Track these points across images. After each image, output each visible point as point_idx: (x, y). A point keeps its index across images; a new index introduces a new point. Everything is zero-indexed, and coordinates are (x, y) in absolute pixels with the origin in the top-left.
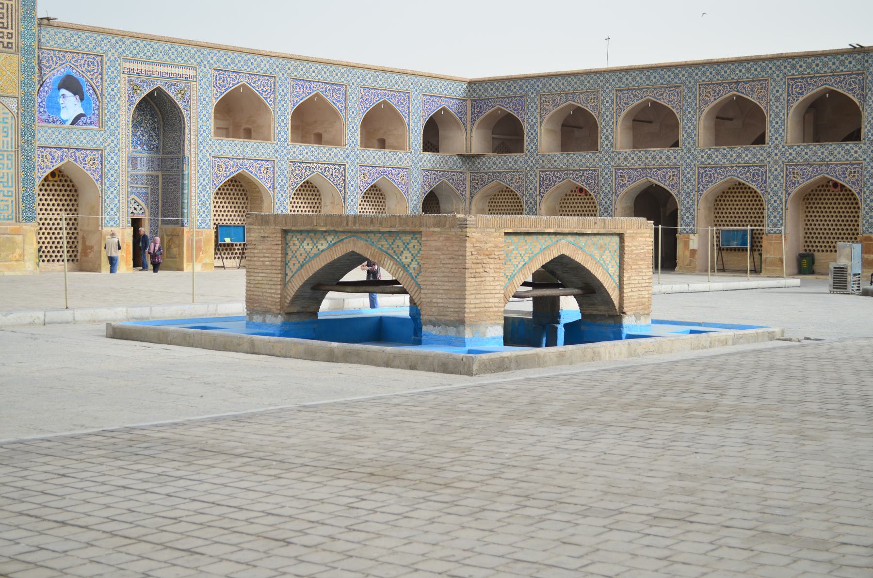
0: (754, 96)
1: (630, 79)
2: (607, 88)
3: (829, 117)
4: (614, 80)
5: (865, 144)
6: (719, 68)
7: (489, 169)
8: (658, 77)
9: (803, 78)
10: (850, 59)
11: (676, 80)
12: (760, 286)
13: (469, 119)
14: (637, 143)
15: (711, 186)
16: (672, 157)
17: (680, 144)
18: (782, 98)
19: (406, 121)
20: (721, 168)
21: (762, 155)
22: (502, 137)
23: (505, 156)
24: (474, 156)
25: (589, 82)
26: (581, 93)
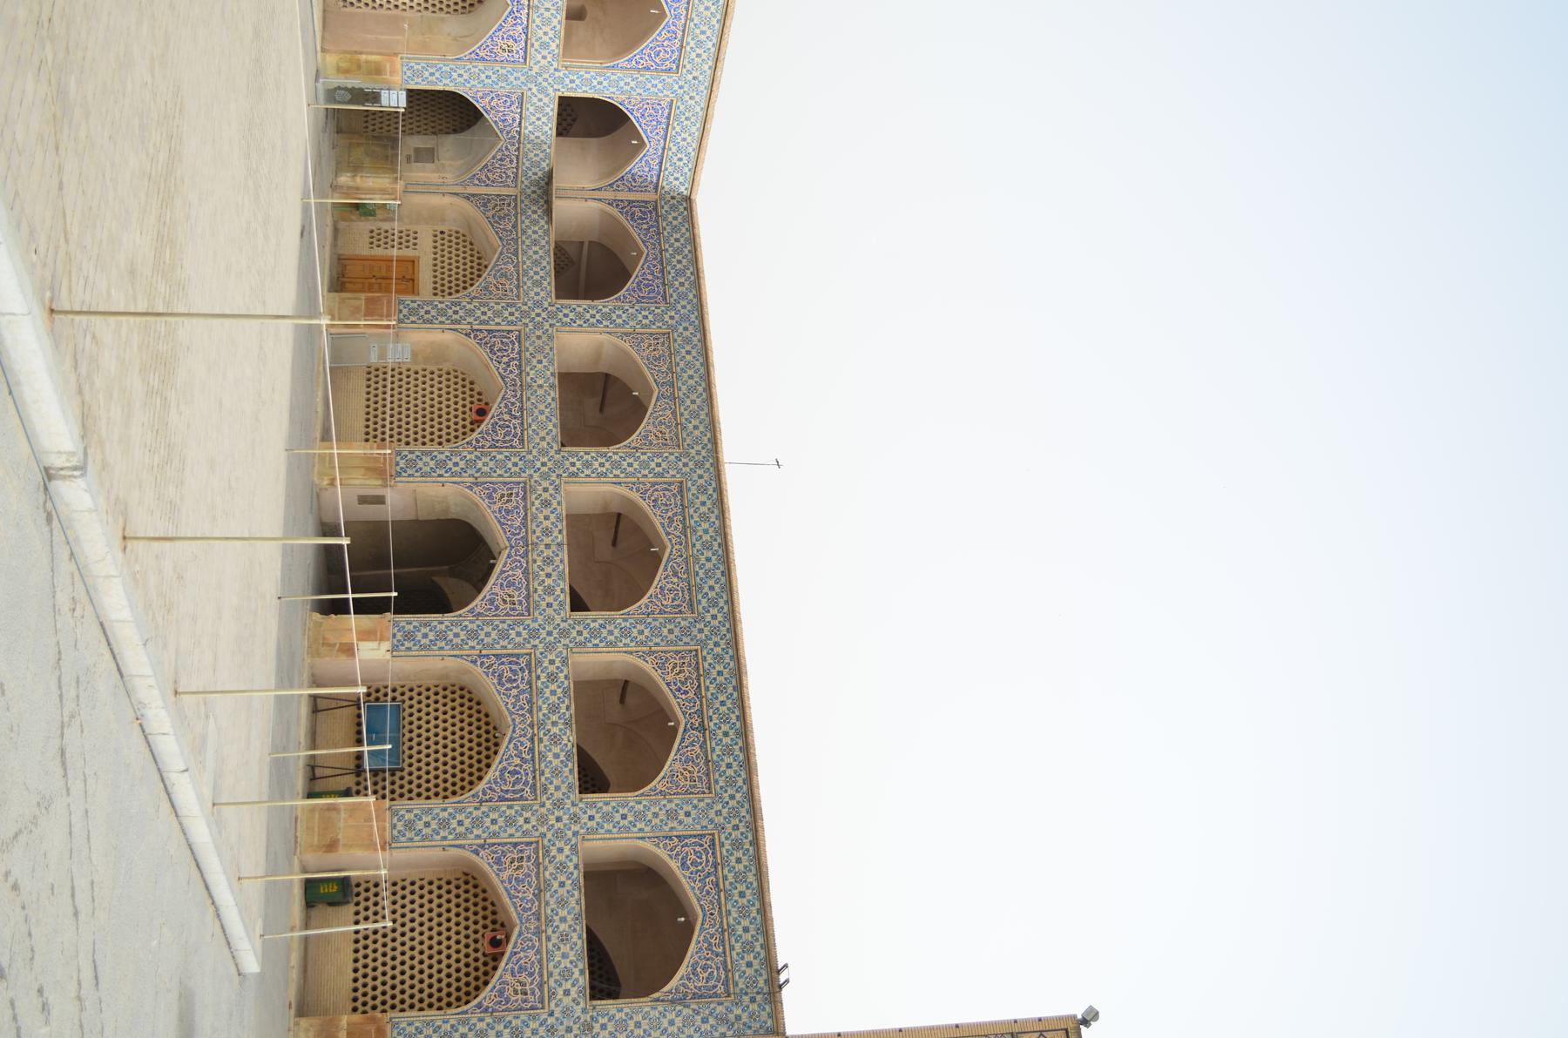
0: (678, 766)
1: (704, 509)
2: (685, 465)
3: (639, 928)
4: (701, 477)
5: (584, 1011)
6: (730, 690)
7: (524, 232)
8: (709, 565)
9: (715, 865)
10: (756, 963)
11: (704, 602)
12: (225, 913)
13: (620, 196)
14: (579, 524)
15: (490, 683)
16: (550, 599)
17: (578, 615)
18: (675, 824)
19: (622, 62)
20: (530, 702)
21: (557, 788)
22: (584, 259)
23: (548, 264)
24: (549, 203)
25: (696, 427)
26: (674, 413)
